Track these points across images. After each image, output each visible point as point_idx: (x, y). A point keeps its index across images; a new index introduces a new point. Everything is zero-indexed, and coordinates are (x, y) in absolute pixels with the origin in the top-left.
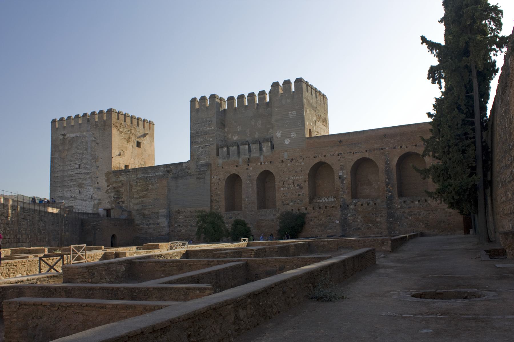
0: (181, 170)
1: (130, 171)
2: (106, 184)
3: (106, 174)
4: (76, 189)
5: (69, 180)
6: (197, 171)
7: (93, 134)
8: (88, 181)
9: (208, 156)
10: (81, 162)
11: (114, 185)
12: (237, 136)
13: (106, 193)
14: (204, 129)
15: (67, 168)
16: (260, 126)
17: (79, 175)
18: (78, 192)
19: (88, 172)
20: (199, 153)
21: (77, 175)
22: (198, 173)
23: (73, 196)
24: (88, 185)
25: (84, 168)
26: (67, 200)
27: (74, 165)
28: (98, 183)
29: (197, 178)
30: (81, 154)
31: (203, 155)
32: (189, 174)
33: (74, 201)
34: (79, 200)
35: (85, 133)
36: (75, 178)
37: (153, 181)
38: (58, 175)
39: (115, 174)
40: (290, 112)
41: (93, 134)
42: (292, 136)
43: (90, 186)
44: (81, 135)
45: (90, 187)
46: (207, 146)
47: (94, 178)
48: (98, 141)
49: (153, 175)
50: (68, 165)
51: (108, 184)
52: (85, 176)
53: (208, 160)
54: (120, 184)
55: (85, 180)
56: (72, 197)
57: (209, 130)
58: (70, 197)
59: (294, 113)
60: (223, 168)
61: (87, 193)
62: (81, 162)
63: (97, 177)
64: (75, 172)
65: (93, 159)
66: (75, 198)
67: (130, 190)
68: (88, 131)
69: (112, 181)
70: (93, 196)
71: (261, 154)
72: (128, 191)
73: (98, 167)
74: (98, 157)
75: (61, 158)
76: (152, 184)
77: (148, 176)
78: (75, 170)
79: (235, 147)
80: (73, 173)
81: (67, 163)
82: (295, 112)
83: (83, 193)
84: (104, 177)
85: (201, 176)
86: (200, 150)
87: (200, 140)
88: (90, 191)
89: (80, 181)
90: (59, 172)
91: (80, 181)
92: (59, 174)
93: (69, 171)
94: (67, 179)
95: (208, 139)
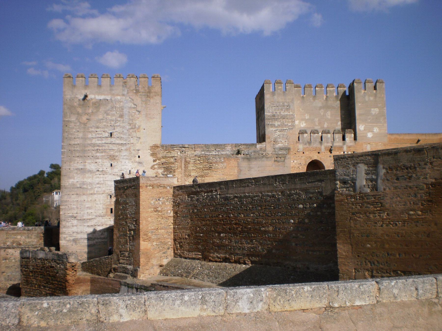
0: (255, 152)
1: (186, 146)
2: (151, 159)
3: (151, 147)
4: (104, 161)
5: (93, 150)
6: (274, 154)
7: (133, 100)
8: (124, 153)
9: (287, 140)
10: (114, 131)
11: (163, 160)
12: (305, 123)
13: (151, 168)
14: (281, 113)
15: (90, 136)
16: (329, 117)
17: (111, 146)
18: (110, 165)
19: (125, 142)
20: (276, 136)
21: (107, 145)
22: (276, 156)
23: (101, 170)
24: (125, 157)
25: (118, 138)
26: (91, 173)
27: (103, 133)
28: (139, 157)
29: (275, 161)
30: (113, 121)
31: (280, 138)
32: (264, 156)
33: (102, 176)
34: (110, 174)
35: (119, 97)
36: (104, 148)
37: (218, 159)
38: (76, 143)
39: (165, 148)
40: (373, 109)
41: (133, 100)
42: (375, 130)
43: (127, 159)
44: (113, 99)
45: (127, 161)
46: (286, 130)
47: (134, 150)
48: (139, 109)
49: (217, 153)
50: (92, 132)
51: (154, 159)
52: (120, 147)
53: (286, 144)
54: (172, 160)
55: (120, 151)
56: (98, 171)
57: (287, 115)
58: (95, 170)
59: (377, 110)
60: (303, 153)
61: (123, 167)
62: (114, 131)
63: (138, 150)
64: (103, 142)
65: (131, 129)
66: (104, 172)
67: (186, 167)
68: (123, 95)
69: (160, 156)
70: (131, 171)
71: (344, 144)
72: (183, 168)
73: (140, 138)
74: (139, 127)
75: (81, 123)
76: (216, 162)
77: (210, 154)
78: (104, 139)
79: (316, 134)
80: (100, 142)
81: (91, 130)
82: (377, 109)
83: (116, 167)
84: (149, 151)
85: (279, 159)
86: (277, 133)
87: (277, 123)
88: (126, 165)
89: (112, 153)
90: (77, 139)
91: (112, 153)
92: (78, 141)
93: (94, 139)
94: (90, 148)
95: (286, 124)
